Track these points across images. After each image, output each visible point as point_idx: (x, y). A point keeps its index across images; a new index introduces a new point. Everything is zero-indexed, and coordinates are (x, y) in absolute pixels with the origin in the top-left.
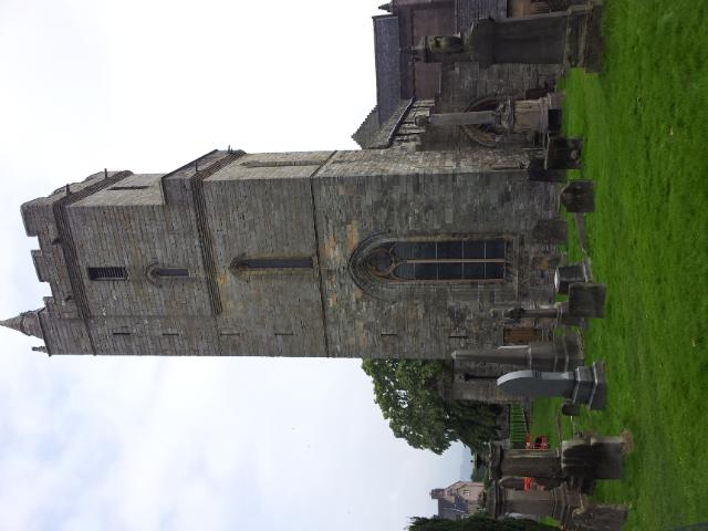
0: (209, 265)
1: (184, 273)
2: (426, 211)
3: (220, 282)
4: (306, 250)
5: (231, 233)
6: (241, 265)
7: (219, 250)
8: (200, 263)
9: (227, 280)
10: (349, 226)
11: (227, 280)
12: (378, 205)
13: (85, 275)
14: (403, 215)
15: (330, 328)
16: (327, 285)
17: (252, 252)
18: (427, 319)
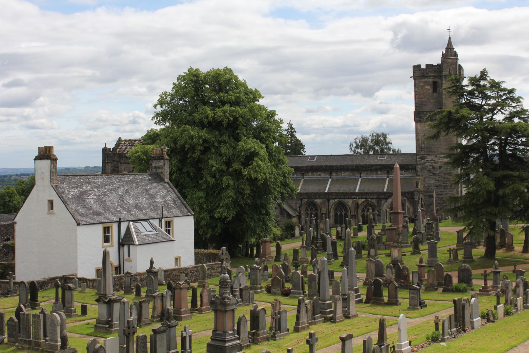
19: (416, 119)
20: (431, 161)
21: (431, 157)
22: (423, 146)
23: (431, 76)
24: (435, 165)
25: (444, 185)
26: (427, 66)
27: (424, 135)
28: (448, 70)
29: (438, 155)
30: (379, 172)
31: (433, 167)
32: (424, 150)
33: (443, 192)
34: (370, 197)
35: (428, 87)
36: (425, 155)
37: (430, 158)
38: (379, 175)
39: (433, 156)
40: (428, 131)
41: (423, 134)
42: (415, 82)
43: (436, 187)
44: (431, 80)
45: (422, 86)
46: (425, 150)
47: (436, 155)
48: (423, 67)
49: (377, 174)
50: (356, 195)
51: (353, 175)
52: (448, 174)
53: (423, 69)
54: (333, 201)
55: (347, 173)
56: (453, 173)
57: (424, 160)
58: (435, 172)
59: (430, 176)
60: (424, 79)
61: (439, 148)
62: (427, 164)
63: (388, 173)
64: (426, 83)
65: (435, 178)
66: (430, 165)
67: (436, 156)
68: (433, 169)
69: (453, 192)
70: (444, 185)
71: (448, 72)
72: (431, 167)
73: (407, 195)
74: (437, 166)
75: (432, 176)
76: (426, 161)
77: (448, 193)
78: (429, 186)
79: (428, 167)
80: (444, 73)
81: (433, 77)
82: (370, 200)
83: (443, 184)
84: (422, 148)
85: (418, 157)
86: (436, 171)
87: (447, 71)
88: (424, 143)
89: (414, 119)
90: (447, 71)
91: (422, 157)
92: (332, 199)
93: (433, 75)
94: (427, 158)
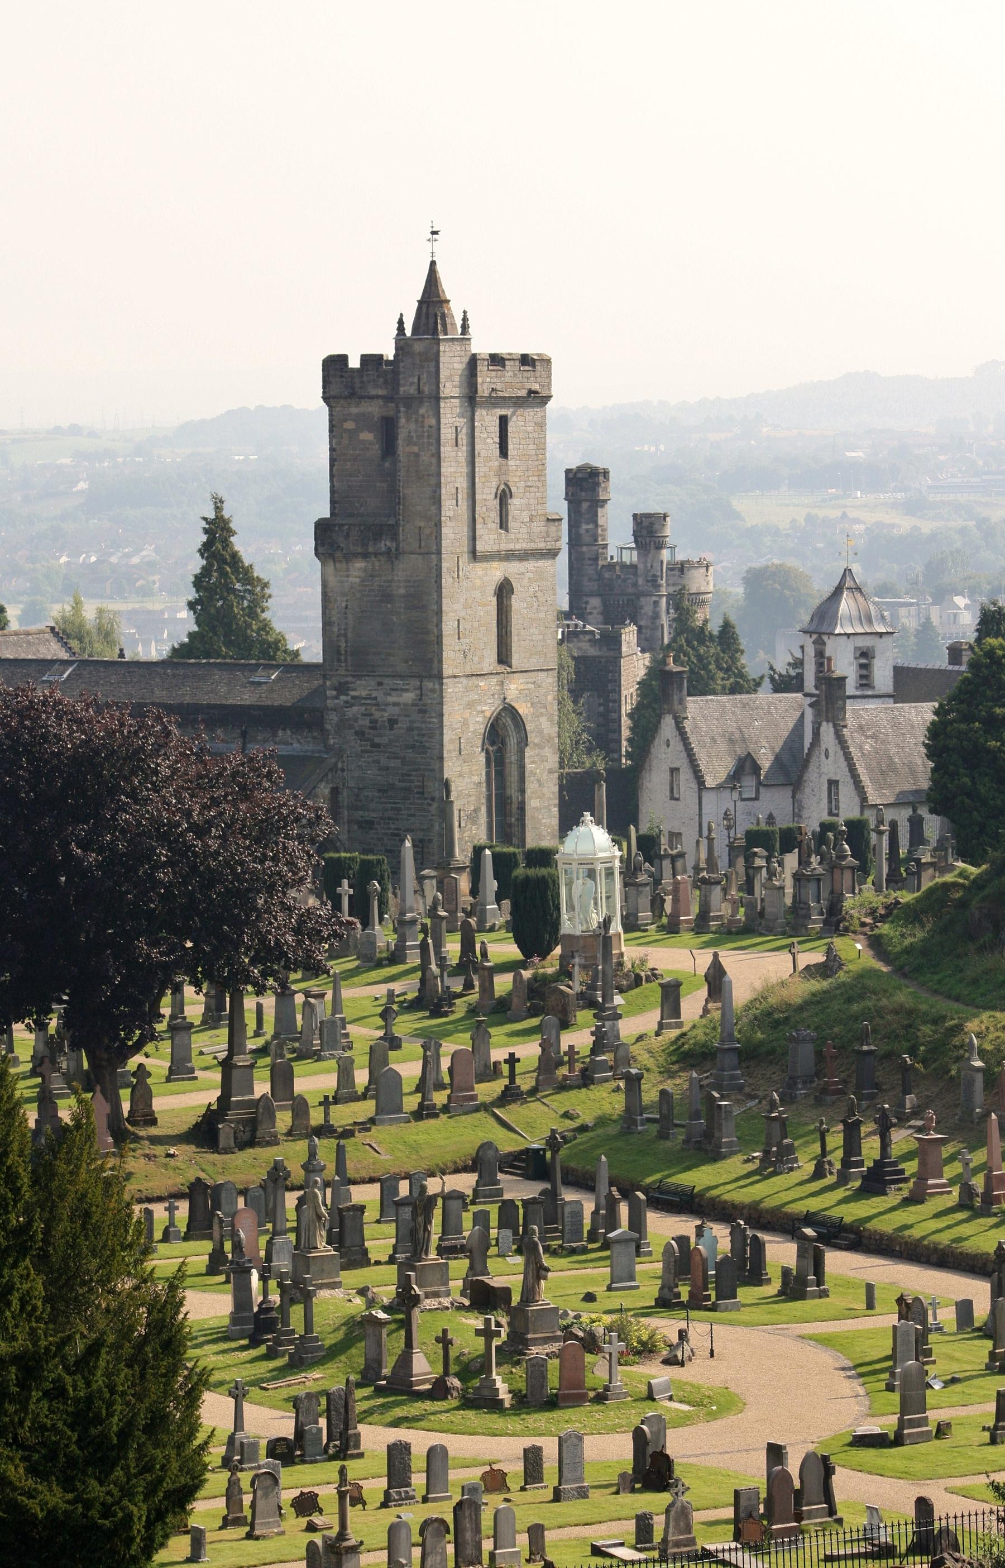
0: (509, 556)
1: (503, 524)
2: (539, 781)
3: (495, 564)
4: (516, 660)
5: (525, 582)
6: (504, 591)
7: (512, 569)
8: (511, 546)
9: (495, 572)
10: (529, 705)
11: (495, 572)
12: (541, 732)
13: (503, 412)
14: (536, 759)
15: (464, 680)
16: (494, 680)
17: (517, 603)
18: (472, 786)
19: (321, 550)
20: (366, 699)
22: (343, 644)
23: (378, 397)
24: (377, 715)
25: (404, 784)
26: (365, 359)
27: (346, 607)
28: (416, 380)
29: (386, 681)
31: (370, 722)
32: (346, 660)
33: (399, 809)
35: (367, 436)
36: (350, 679)
37: (362, 689)
39: (372, 682)
41: (344, 605)
42: (331, 415)
43: (380, 791)
44: (374, 409)
46: (349, 658)
47: (379, 679)
52: (413, 747)
53: (353, 370)
56: (427, 744)
57: (347, 695)
58: (377, 740)
59: (362, 751)
60: (357, 405)
62: (355, 709)
63: (244, 735)
65: (378, 762)
66: (363, 715)
67: (380, 684)
69: (429, 811)
70: (404, 784)
71: (415, 387)
72: (366, 722)
74: (382, 716)
75: (367, 751)
76: (353, 698)
77: (414, 815)
78: (359, 789)
79: (356, 720)
80: (402, 389)
81: (381, 402)
83: (400, 781)
84: (339, 653)
85: (328, 683)
86: (380, 736)
87: (412, 384)
88: (345, 635)
89: (316, 549)
90: (412, 384)
91: (340, 683)
93: (380, 392)
94: (355, 690)
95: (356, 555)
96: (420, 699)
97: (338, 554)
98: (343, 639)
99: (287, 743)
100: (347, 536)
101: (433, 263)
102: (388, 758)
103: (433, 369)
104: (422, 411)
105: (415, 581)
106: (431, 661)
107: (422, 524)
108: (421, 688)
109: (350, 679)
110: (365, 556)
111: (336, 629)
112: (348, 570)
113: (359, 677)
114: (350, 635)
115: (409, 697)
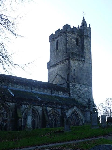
21: (78, 85)
24: (80, 92)
29: (82, 85)
30: (45, 90)
34: (56, 106)
36: (75, 83)
37: (78, 86)
38: (45, 92)
39: (80, 85)
40: (77, 68)
45: (71, 38)
46: (75, 79)
47: (81, 85)
48: (72, 27)
49: (44, 91)
50: (45, 104)
51: (26, 89)
54: (25, 106)
55: (21, 86)
58: (80, 97)
61: (83, 80)
64: (73, 38)
67: (81, 86)
68: (79, 94)
73: (81, 108)
75: (78, 99)
76: (76, 87)
79: (76, 92)
82: (56, 109)
84: (73, 78)
90: (86, 34)
91: (73, 84)
92: (25, 104)
93: (77, 34)
94: (76, 86)
95: (77, 60)
96: (88, 90)
97: (74, 59)
98: (74, 76)
99: (61, 95)
100: (76, 56)
101: (84, 17)
102: (83, 100)
103: (90, 33)
104: (88, 39)
105: (87, 68)
106: (90, 83)
107: (88, 58)
108: (88, 88)
109: (75, 83)
110: (79, 60)
111: (73, 73)
112: (75, 62)
113: (77, 83)
114: (75, 75)
115: (86, 89)
